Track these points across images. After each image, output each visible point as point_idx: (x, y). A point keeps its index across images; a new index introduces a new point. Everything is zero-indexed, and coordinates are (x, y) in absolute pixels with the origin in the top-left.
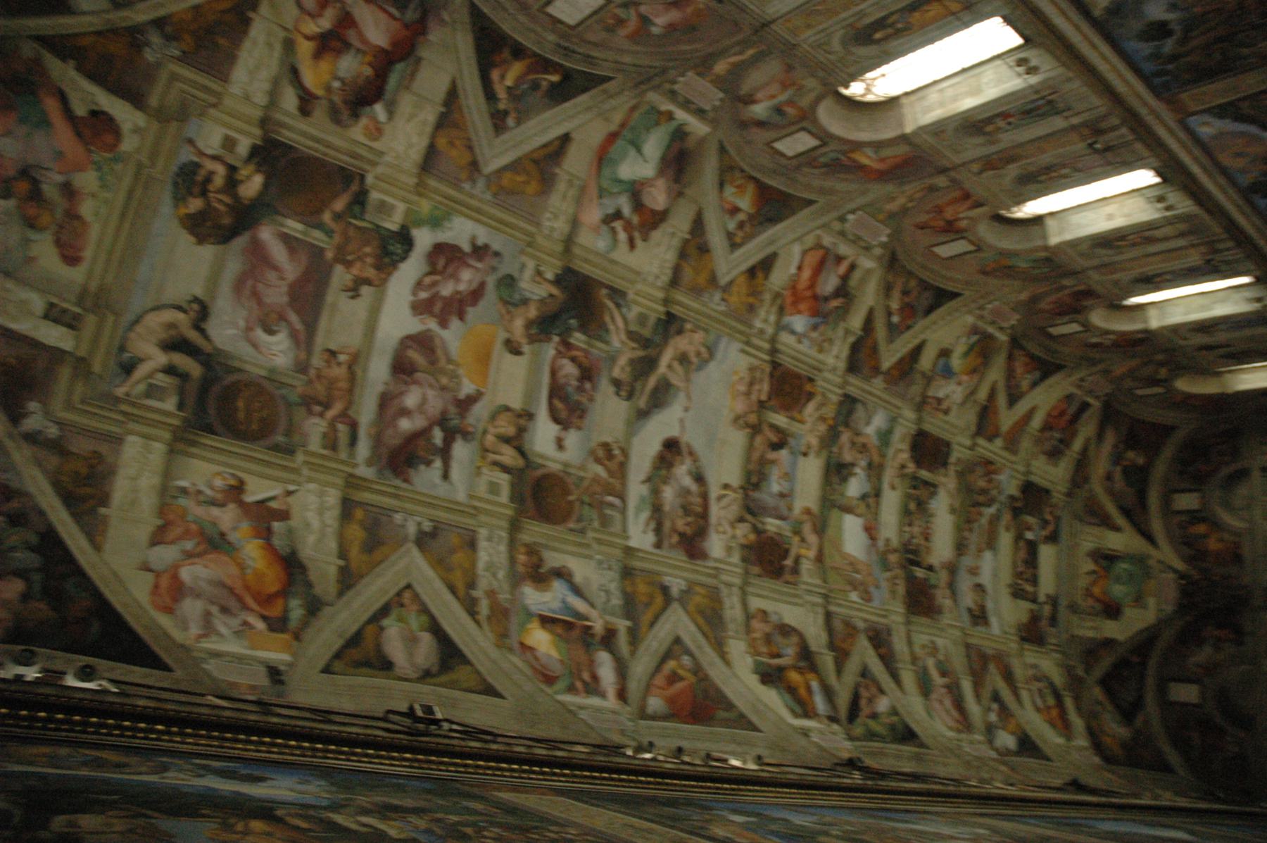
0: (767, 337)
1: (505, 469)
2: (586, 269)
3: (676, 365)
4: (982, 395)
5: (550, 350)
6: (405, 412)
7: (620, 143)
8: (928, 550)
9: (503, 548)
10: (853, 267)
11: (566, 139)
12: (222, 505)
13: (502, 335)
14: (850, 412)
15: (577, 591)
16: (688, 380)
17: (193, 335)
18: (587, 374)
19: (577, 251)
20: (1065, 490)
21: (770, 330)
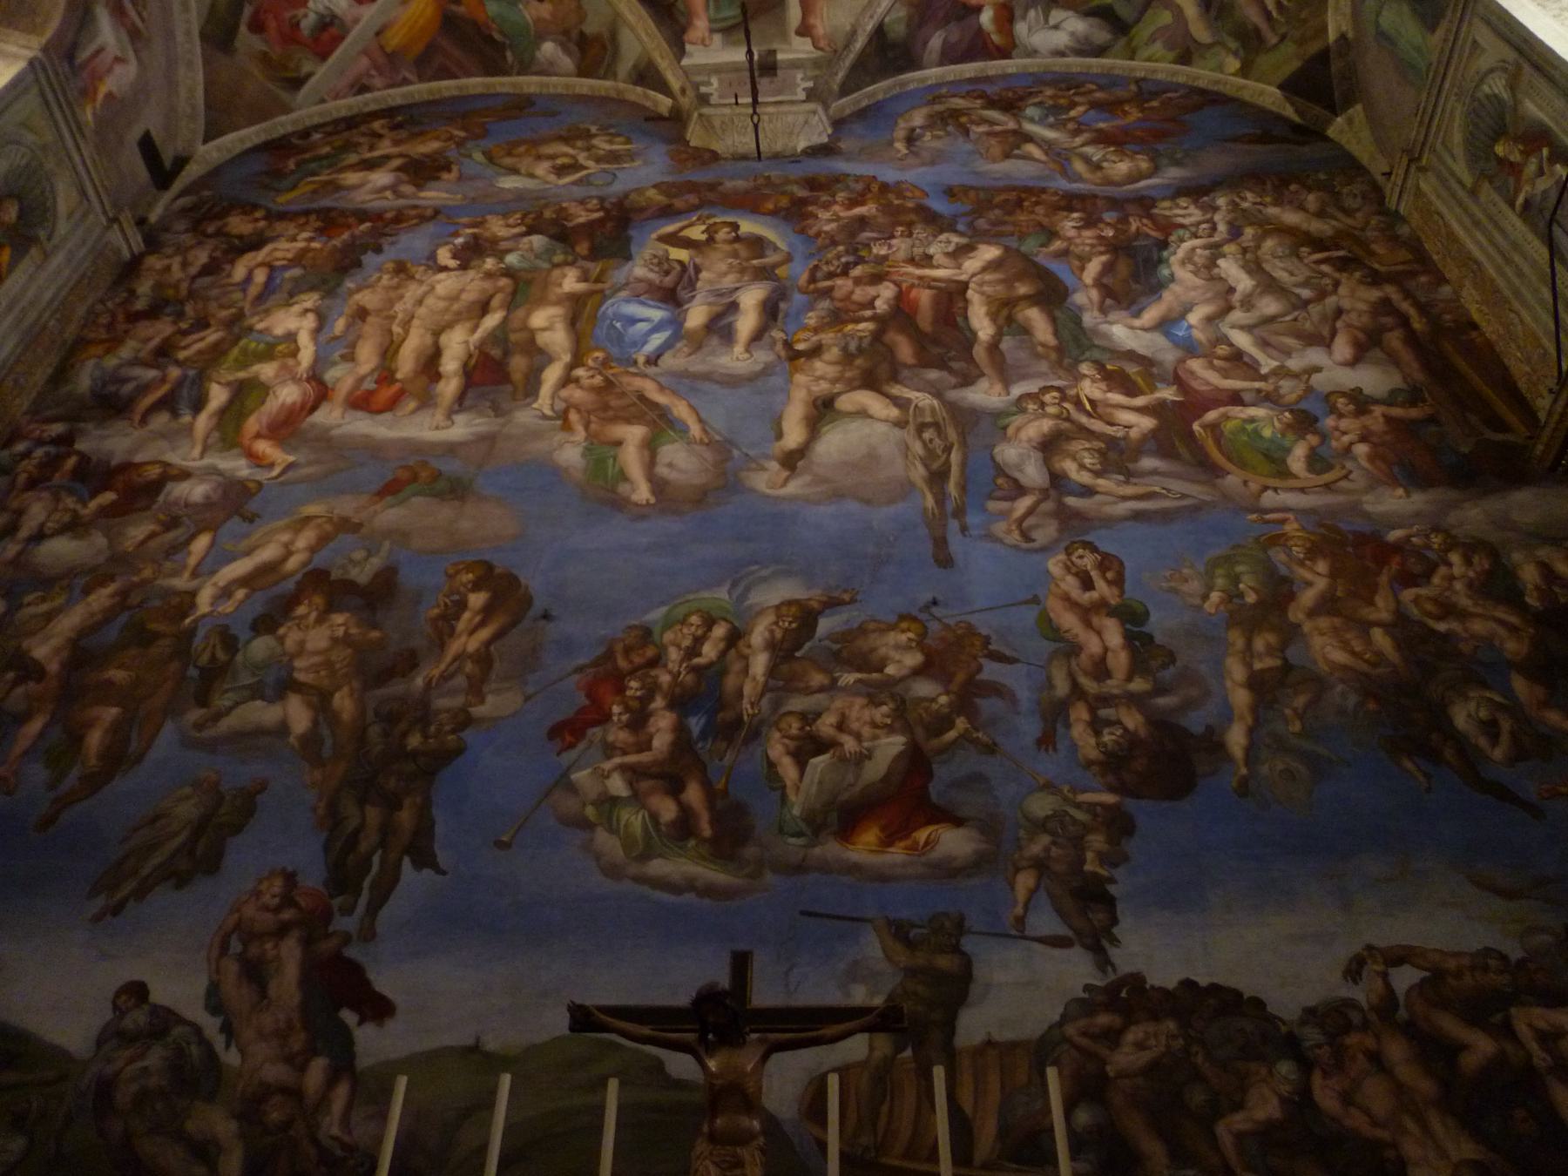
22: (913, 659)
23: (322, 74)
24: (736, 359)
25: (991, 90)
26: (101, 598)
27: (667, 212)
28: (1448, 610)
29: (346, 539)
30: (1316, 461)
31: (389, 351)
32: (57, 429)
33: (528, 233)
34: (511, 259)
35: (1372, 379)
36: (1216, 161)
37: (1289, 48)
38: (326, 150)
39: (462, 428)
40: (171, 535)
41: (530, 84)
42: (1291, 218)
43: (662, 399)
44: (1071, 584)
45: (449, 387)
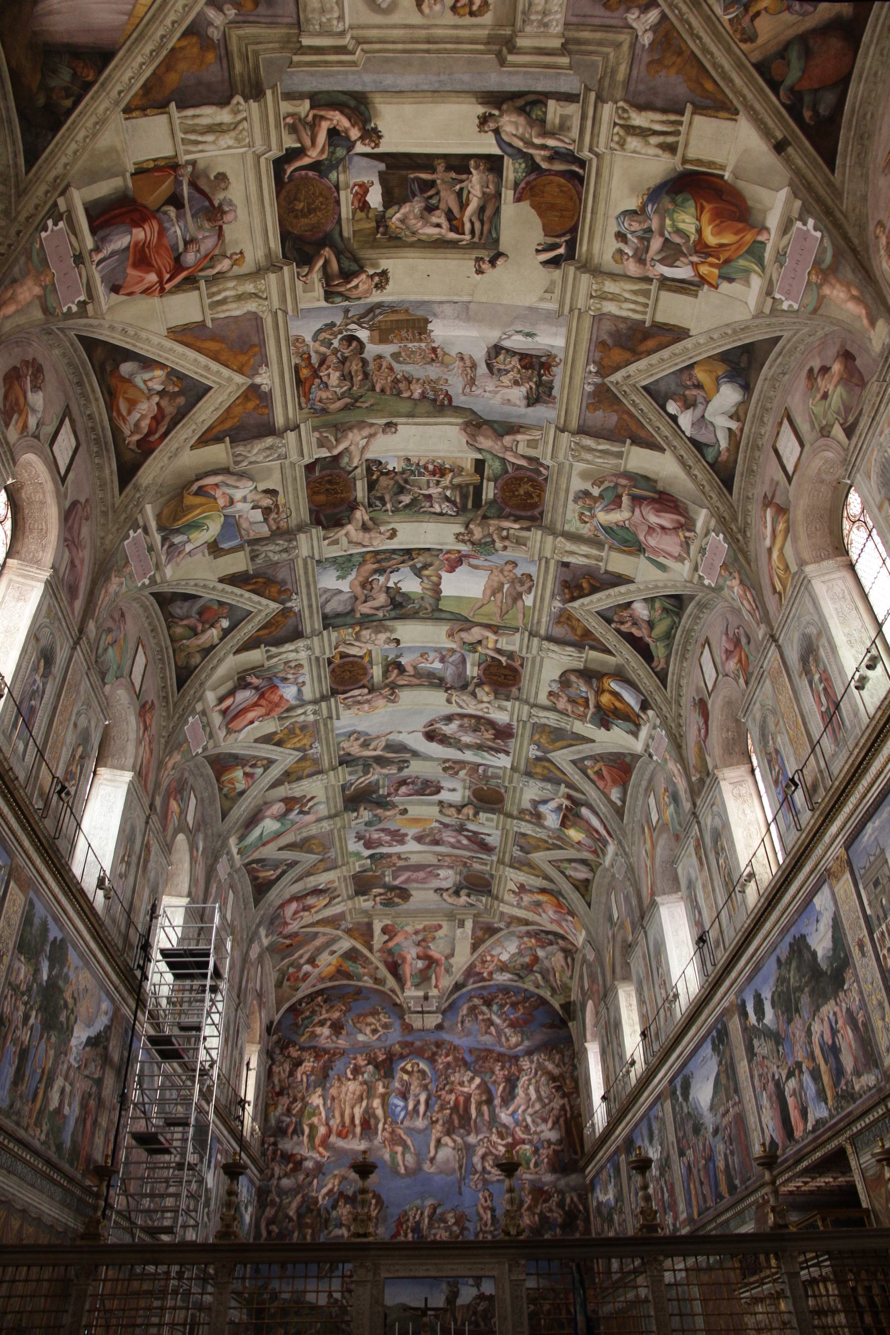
0: (317, 708)
1: (476, 814)
2: (340, 805)
3: (371, 747)
4: (218, 453)
5: (396, 799)
6: (459, 842)
7: (264, 840)
8: (457, 470)
9: (523, 823)
10: (221, 700)
11: (280, 849)
12: (522, 898)
13: (399, 817)
14: (338, 615)
15: (545, 802)
16: (378, 737)
17: (451, 891)
18: (403, 782)
19: (333, 812)
20: (254, 105)
21: (310, 708)
22: (453, 1220)
23: (303, 986)
24: (420, 1123)
25: (485, 993)
26: (299, 1198)
27: (402, 1057)
28: (551, 1210)
29: (345, 1182)
30: (536, 1165)
31: (342, 1115)
32: (272, 1140)
33: (369, 1064)
34: (366, 1076)
35: (553, 1136)
36: (539, 1037)
37: (562, 997)
38: (308, 1013)
39: (363, 1146)
40: (309, 1179)
41: (360, 984)
42: (550, 1066)
43: (404, 1137)
44: (483, 1200)
45: (358, 1130)
